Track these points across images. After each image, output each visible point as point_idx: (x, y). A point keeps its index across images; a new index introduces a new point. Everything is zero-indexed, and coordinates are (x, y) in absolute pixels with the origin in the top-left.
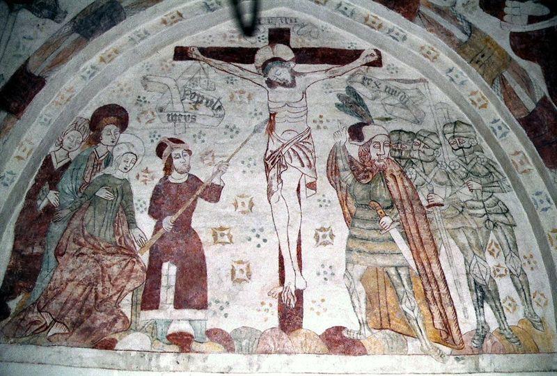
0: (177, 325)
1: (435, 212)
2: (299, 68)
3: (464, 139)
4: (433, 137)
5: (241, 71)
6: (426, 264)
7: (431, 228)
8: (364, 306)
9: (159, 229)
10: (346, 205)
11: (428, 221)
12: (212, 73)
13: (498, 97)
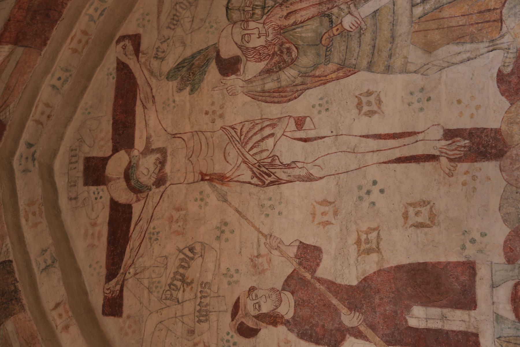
0: (501, 306)
2: (139, 144)
5: (141, 222)
8: (468, 46)
9: (360, 332)
10: (326, 76)
12: (144, 261)
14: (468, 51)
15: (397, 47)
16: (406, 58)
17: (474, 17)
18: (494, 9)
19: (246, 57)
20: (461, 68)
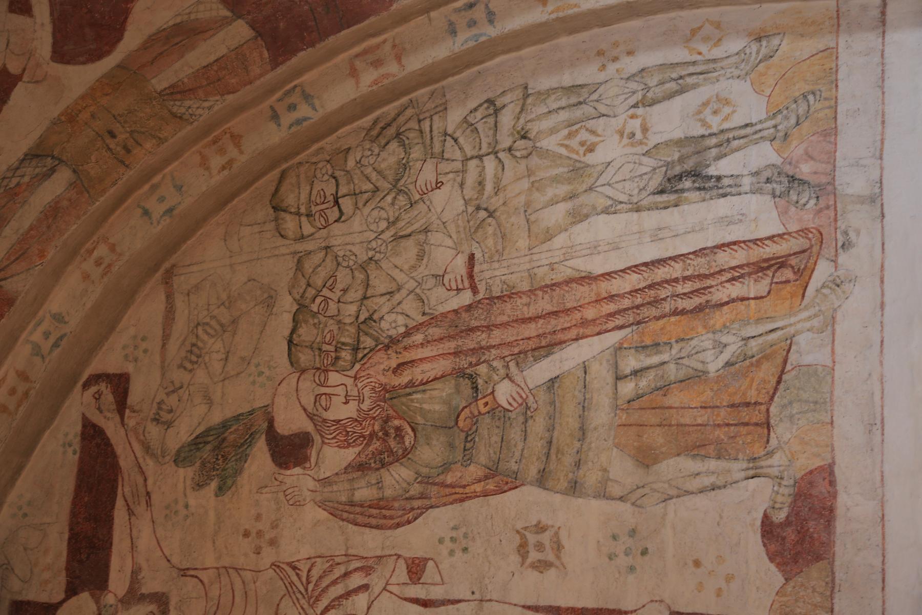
1: (487, 275)
2: (118, 583)
3: (314, 192)
4: (308, 266)
6: (612, 307)
7: (525, 286)
8: (713, 464)
10: (464, 487)
11: (510, 295)
13: (216, 108)
14: (713, 473)
15: (590, 449)
16: (605, 470)
17: (723, 412)
18: (755, 403)
19: (322, 437)
20: (700, 501)
